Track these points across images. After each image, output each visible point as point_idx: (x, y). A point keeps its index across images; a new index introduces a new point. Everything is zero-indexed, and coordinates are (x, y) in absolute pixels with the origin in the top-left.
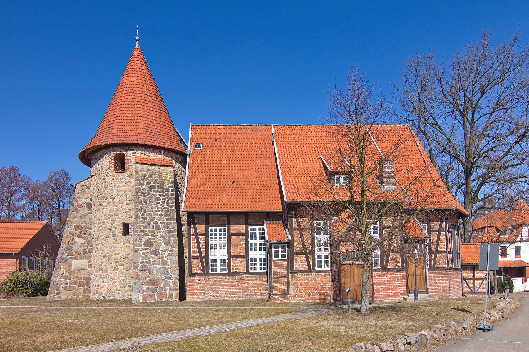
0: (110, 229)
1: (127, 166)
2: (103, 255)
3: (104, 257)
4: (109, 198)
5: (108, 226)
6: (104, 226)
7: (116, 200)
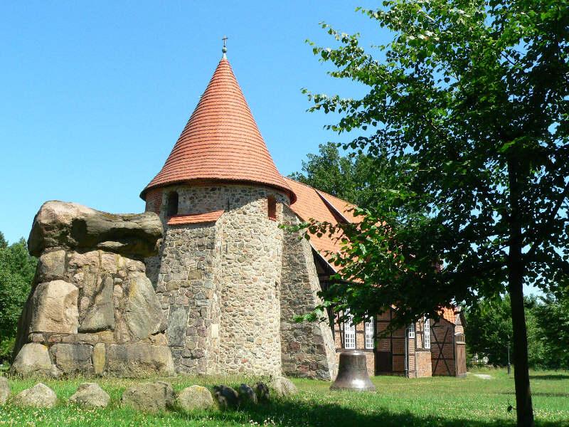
0: (265, 289)
1: (277, 214)
2: (255, 321)
3: (258, 324)
4: (263, 249)
5: (263, 284)
6: (256, 284)
7: (271, 253)
